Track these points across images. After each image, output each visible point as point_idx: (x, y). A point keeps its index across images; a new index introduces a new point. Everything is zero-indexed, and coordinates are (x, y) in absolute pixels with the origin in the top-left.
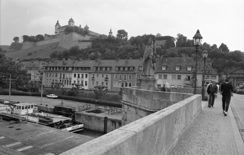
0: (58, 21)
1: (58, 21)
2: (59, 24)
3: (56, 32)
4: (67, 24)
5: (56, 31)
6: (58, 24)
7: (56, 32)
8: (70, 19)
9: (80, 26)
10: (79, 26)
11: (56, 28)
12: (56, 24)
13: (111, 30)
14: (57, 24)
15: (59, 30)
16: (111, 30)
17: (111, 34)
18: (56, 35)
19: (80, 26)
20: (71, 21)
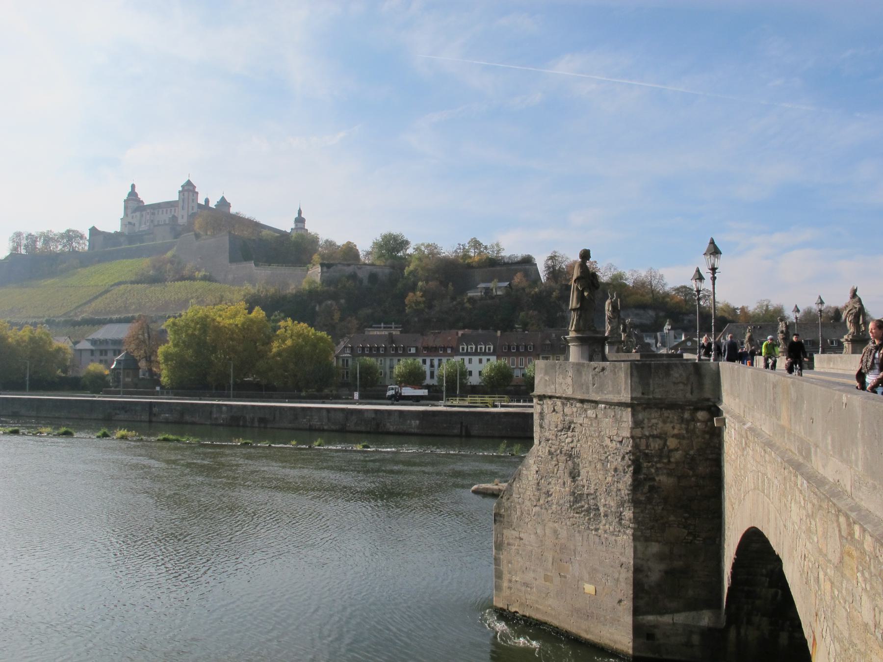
0: (133, 186)
1: (133, 186)
2: (136, 195)
3: (130, 223)
4: (175, 197)
6: (133, 195)
7: (125, 222)
8: (183, 182)
9: (207, 201)
11: (126, 208)
12: (125, 197)
13: (300, 212)
15: (142, 216)
16: (300, 212)
17: (300, 225)
20: (189, 189)
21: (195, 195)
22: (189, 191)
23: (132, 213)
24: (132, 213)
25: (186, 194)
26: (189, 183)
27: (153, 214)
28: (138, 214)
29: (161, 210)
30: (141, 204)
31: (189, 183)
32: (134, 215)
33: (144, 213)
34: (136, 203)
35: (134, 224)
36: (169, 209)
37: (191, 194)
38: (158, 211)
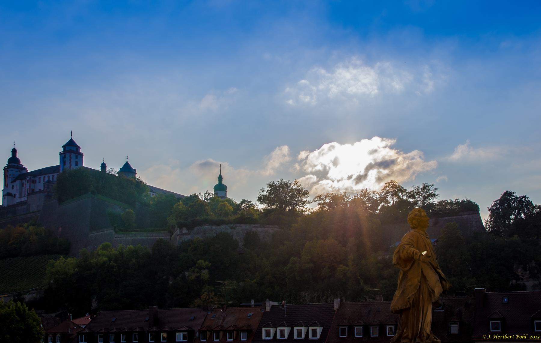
2: (18, 161)
5: (10, 190)
9: (104, 166)
10: (99, 169)
12: (5, 164)
14: (10, 161)
15: (22, 185)
18: (9, 207)
19: (104, 166)
21: (79, 156)
22: (70, 152)
23: (12, 182)
24: (12, 182)
25: (68, 155)
26: (71, 143)
27: (34, 182)
28: (18, 182)
29: (42, 177)
30: (24, 172)
31: (71, 143)
32: (14, 184)
33: (23, 181)
34: (17, 170)
35: (15, 195)
36: (51, 175)
37: (73, 156)
38: (40, 178)
